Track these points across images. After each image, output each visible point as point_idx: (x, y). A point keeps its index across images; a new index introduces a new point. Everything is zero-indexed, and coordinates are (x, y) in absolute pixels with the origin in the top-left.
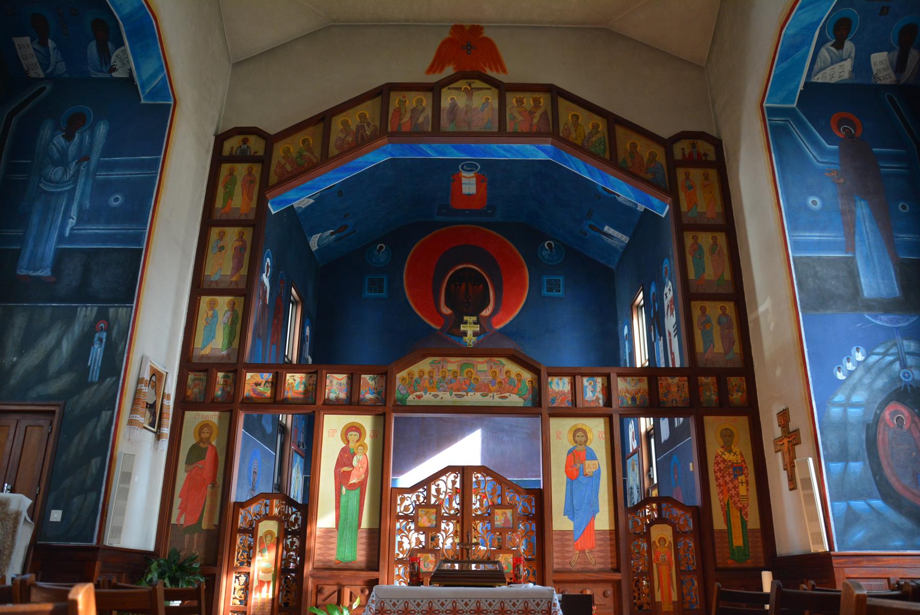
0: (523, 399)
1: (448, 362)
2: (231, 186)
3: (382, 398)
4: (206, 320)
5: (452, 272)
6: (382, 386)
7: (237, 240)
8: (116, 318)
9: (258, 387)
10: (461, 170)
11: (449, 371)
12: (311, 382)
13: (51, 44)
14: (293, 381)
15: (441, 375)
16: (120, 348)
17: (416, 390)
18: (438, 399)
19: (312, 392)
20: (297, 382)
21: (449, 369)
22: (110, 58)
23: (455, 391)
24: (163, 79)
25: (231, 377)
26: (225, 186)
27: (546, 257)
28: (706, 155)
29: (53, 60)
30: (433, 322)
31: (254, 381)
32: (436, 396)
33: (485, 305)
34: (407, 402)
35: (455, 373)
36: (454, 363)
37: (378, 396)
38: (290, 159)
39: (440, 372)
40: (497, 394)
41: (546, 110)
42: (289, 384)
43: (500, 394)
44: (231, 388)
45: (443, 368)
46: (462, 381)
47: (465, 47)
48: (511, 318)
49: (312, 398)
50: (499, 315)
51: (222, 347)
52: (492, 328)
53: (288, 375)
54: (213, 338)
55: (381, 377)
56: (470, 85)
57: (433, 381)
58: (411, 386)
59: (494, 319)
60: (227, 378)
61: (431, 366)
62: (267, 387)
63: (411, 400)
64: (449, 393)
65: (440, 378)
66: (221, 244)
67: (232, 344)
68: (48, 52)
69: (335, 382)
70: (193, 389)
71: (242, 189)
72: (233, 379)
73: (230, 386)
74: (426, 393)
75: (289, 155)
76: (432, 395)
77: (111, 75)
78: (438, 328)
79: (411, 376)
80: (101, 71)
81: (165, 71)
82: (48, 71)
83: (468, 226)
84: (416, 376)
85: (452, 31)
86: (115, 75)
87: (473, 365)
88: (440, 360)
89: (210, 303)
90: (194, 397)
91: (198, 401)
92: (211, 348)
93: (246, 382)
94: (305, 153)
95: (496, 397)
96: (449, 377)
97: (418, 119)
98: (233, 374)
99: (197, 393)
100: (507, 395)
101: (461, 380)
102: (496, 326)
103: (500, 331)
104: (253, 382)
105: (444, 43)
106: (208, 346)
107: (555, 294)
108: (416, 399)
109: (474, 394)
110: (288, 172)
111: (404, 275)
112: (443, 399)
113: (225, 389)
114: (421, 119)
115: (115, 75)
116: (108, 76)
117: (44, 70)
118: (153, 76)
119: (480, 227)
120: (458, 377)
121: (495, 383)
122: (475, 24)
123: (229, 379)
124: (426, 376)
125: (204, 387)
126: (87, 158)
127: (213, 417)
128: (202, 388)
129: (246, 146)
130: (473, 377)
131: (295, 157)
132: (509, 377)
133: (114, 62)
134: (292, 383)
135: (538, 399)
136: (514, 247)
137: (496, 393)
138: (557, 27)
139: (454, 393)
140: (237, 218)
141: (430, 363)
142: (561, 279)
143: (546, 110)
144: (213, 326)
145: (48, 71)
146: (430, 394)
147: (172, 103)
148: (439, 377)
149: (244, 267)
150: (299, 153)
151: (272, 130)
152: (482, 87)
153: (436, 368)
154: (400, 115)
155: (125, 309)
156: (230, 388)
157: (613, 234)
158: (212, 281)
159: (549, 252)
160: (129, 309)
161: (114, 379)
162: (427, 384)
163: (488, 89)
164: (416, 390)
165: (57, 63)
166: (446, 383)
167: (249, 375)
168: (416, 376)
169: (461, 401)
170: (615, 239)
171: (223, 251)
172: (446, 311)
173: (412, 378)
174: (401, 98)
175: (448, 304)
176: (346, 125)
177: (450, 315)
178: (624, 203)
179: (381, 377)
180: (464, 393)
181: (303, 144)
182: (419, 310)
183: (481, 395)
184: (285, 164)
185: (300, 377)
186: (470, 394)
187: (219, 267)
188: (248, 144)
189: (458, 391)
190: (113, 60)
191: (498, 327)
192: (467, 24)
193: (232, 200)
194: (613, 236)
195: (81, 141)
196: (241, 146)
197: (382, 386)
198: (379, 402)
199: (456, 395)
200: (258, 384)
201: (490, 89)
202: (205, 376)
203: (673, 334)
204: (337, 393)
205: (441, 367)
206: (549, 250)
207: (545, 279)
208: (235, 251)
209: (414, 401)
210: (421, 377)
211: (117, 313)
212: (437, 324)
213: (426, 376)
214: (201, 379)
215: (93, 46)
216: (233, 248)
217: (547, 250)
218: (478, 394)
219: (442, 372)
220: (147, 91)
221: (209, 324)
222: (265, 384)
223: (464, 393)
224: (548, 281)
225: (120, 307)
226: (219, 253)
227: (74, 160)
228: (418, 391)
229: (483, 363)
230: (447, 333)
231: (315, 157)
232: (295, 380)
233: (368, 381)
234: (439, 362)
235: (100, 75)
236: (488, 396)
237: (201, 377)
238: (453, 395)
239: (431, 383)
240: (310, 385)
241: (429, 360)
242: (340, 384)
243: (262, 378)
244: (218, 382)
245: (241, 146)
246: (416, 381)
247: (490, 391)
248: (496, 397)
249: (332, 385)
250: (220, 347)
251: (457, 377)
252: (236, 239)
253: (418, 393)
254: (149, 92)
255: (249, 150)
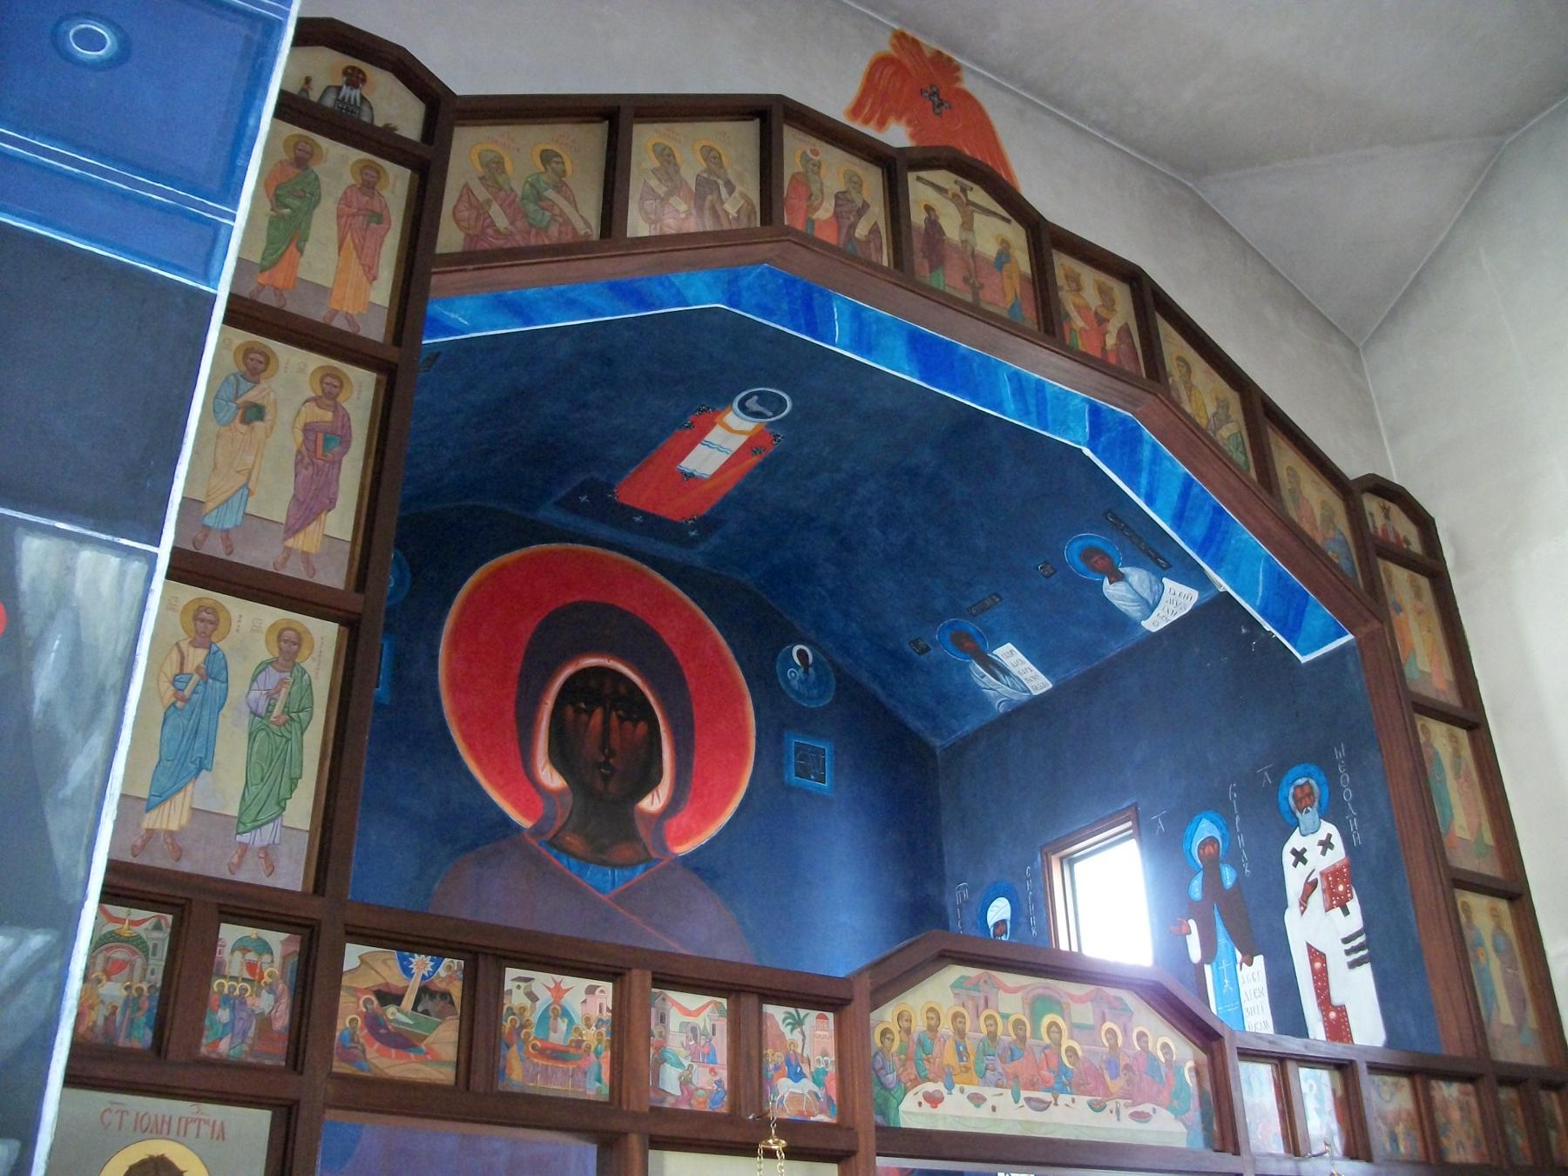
0: (1185, 1124)
1: (999, 988)
2: (296, 203)
3: (829, 1099)
4: (174, 682)
5: (568, 671)
6: (825, 1054)
7: (315, 400)
8: (63, 595)
9: (391, 1011)
10: (735, 405)
11: (1005, 1017)
12: (595, 1014)
14: (528, 1003)
15: (985, 1031)
16: (80, 768)
17: (923, 1074)
18: (986, 1107)
19: (598, 1054)
20: (540, 1006)
21: (1003, 1010)
23: (1026, 1088)
25: (278, 950)
26: (277, 197)
27: (795, 683)
28: (1408, 543)
30: (515, 805)
31: (373, 981)
32: (977, 1100)
33: (648, 783)
34: (901, 1114)
35: (1018, 1024)
36: (1014, 991)
37: (816, 1089)
38: (502, 193)
39: (982, 1018)
40: (1126, 1106)
41: (1126, 324)
42: (510, 1009)
43: (1133, 1105)
44: (276, 1001)
45: (987, 1006)
46: (1039, 1056)
47: (927, 95)
48: (712, 831)
49: (599, 1080)
50: (683, 819)
51: (241, 814)
52: (666, 850)
53: (511, 973)
54: (202, 765)
55: (819, 1017)
56: (964, 190)
57: (965, 1048)
58: (908, 1059)
59: (674, 825)
60: (260, 954)
61: (956, 995)
62: (426, 1012)
63: (912, 1113)
64: (1009, 1091)
65: (981, 1040)
66: (253, 395)
67: (284, 809)
69: (675, 1020)
70: (99, 981)
71: (338, 224)
72: (285, 958)
73: (271, 989)
74: (950, 1087)
75: (500, 180)
76: (969, 1097)
78: (526, 823)
79: (906, 1024)
83: (615, 555)
84: (919, 1025)
85: (895, 41)
87: (1059, 1003)
88: (979, 977)
89: (196, 618)
90: (101, 1022)
91: (122, 1042)
92: (194, 810)
93: (345, 981)
94: (550, 193)
95: (1125, 1113)
96: (1007, 1036)
97: (853, 226)
98: (283, 936)
99: (120, 1003)
100: (1147, 1108)
101: (1037, 1050)
102: (680, 843)
103: (686, 860)
104: (370, 984)
105: (880, 63)
106: (180, 797)
107: (811, 784)
108: (926, 1106)
109: (1073, 1101)
110: (498, 231)
111: (441, 650)
112: (998, 1115)
113: (249, 1001)
114: (861, 231)
119: (645, 566)
120: (1030, 1041)
121: (1117, 1067)
122: (947, 52)
123: (266, 958)
124: (946, 1028)
125: (158, 979)
127: (192, 1128)
128: (145, 986)
129: (356, 93)
130: (1066, 1042)
131: (519, 193)
132: (1145, 1049)
134: (523, 1009)
135: (1215, 1127)
136: (723, 642)
137: (1122, 1102)
138: (1105, 142)
139: (1024, 1094)
140: (319, 319)
141: (953, 986)
142: (826, 747)
143: (1126, 324)
144: (205, 713)
146: (962, 1091)
148: (982, 1035)
149: (338, 503)
150: (532, 185)
151: (462, 83)
152: (993, 209)
153: (970, 1004)
154: (810, 198)
155: (114, 561)
156: (271, 997)
157: (1010, 667)
158: (207, 528)
159: (800, 673)
160: (137, 567)
161: (37, 941)
162: (950, 1058)
163: (1004, 219)
164: (923, 1074)
166: (1000, 1057)
167: (170, 918)
168: (919, 1025)
169: (1042, 1124)
170: (1007, 680)
171: (258, 424)
172: (551, 779)
173: (908, 1031)
174: (809, 153)
175: (562, 757)
176: (669, 163)
177: (559, 793)
178: (1116, 602)
179: (819, 1017)
180: (1047, 1097)
181: (544, 165)
182: (479, 761)
183: (1091, 1105)
184: (489, 202)
185: (552, 985)
186: (1064, 1098)
187: (242, 479)
188: (365, 90)
189: (1032, 1086)
191: (683, 849)
192: (930, 43)
193: (301, 251)
194: (1006, 672)
196: (339, 89)
197: (825, 1054)
198: (821, 1112)
199: (1028, 1100)
200: (389, 997)
201: (1008, 221)
202: (157, 927)
203: (1337, 961)
204: (686, 1063)
205: (982, 1002)
206: (802, 670)
207: (793, 740)
208: (306, 438)
209: (922, 1114)
210: (933, 1029)
211: (69, 570)
212: (526, 815)
213: (946, 1028)
214: (138, 944)
216: (300, 424)
217: (796, 666)
218: (1083, 1100)
219: (988, 1017)
221: (186, 700)
222: (417, 1001)
223: (1047, 1097)
224: (799, 747)
225: (82, 540)
226: (244, 428)
228: (929, 1080)
229: (1081, 1000)
230: (551, 844)
231: (582, 217)
232: (533, 997)
233: (782, 1027)
234: (975, 984)
236: (1107, 1110)
237: (140, 930)
238: (1022, 1102)
239: (959, 1054)
240: (587, 1020)
241: (955, 973)
242: (694, 1029)
243: (407, 971)
244: (222, 964)
245: (339, 89)
246: (921, 1044)
247: (1108, 1095)
248: (1125, 1113)
249: (666, 1028)
250: (233, 810)
251: (1025, 1037)
252: (311, 394)
253: (930, 1087)
255: (365, 108)
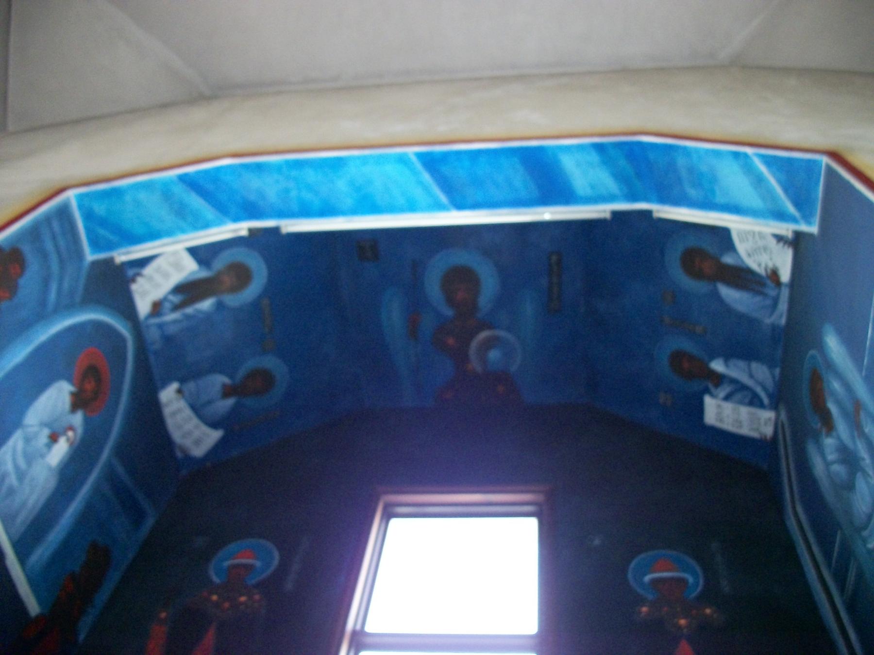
13: (718, 366)
22: (749, 271)
24: (769, 162)
29: (745, 379)
68: (733, 381)
77: (786, 285)
80: (776, 301)
81: (749, 150)
82: (766, 401)
86: (785, 276)
115: (785, 276)
116: (785, 293)
117: (762, 406)
118: (758, 181)
126: (858, 405)
133: (759, 265)
145: (766, 401)
147: (825, 160)
165: (751, 376)
190: (754, 266)
195: (838, 402)
215: (728, 293)
220: (791, 209)
227: (854, 443)
235: (783, 306)
254: (797, 204)
